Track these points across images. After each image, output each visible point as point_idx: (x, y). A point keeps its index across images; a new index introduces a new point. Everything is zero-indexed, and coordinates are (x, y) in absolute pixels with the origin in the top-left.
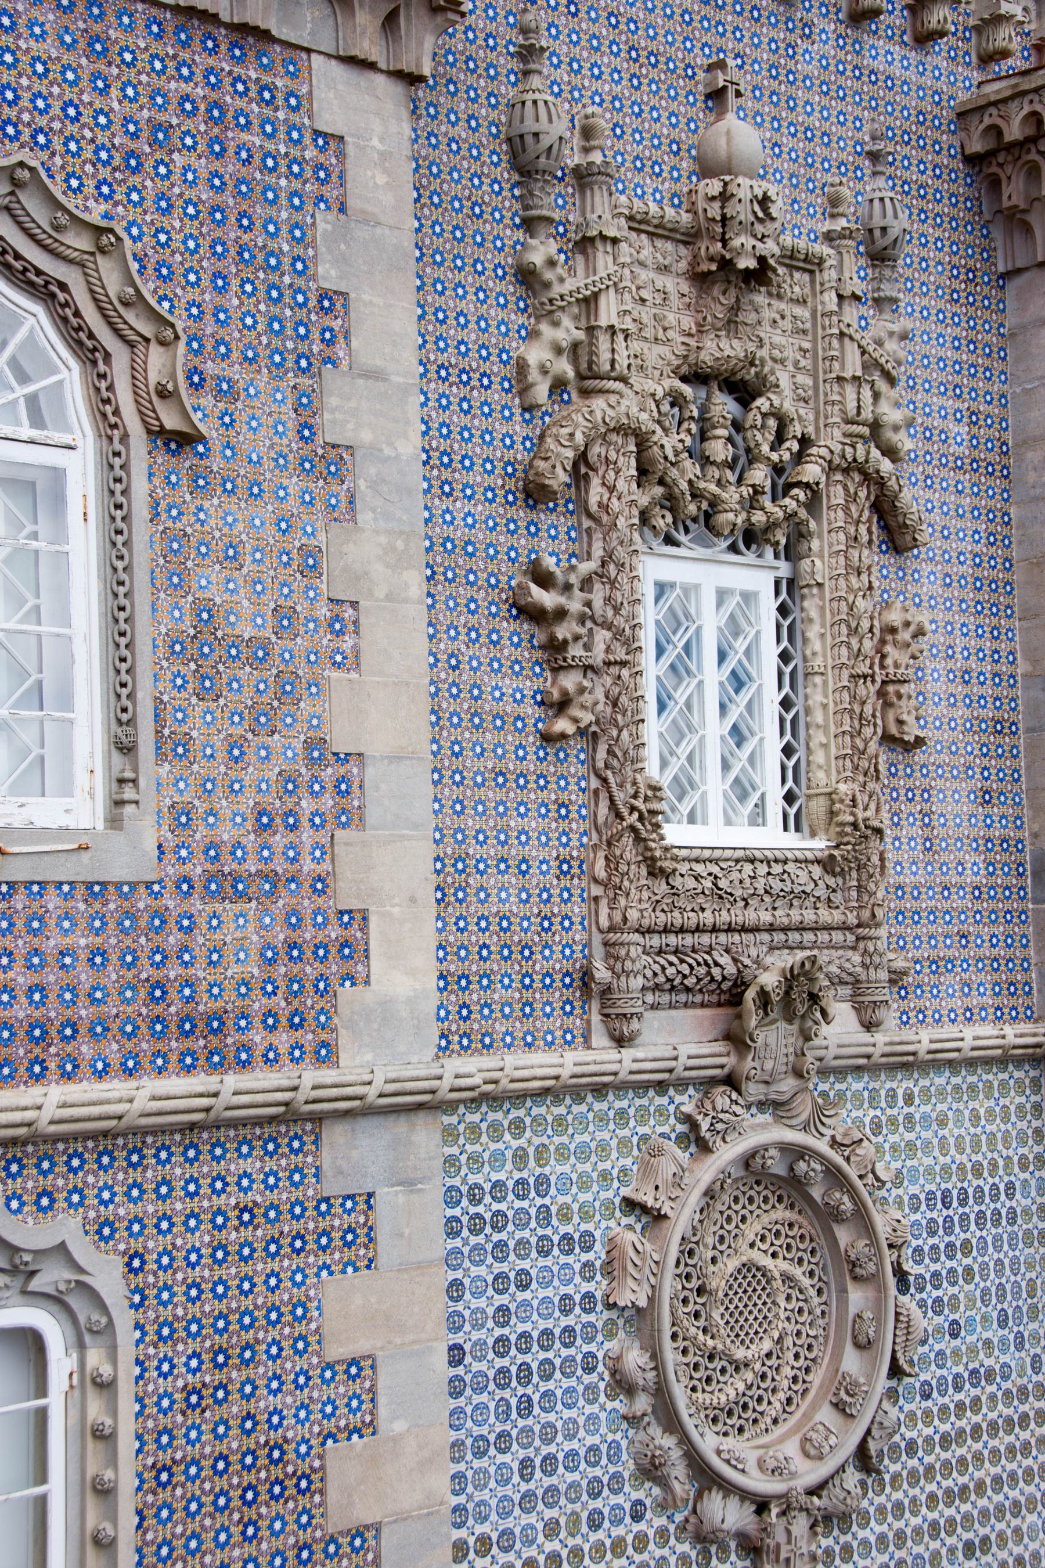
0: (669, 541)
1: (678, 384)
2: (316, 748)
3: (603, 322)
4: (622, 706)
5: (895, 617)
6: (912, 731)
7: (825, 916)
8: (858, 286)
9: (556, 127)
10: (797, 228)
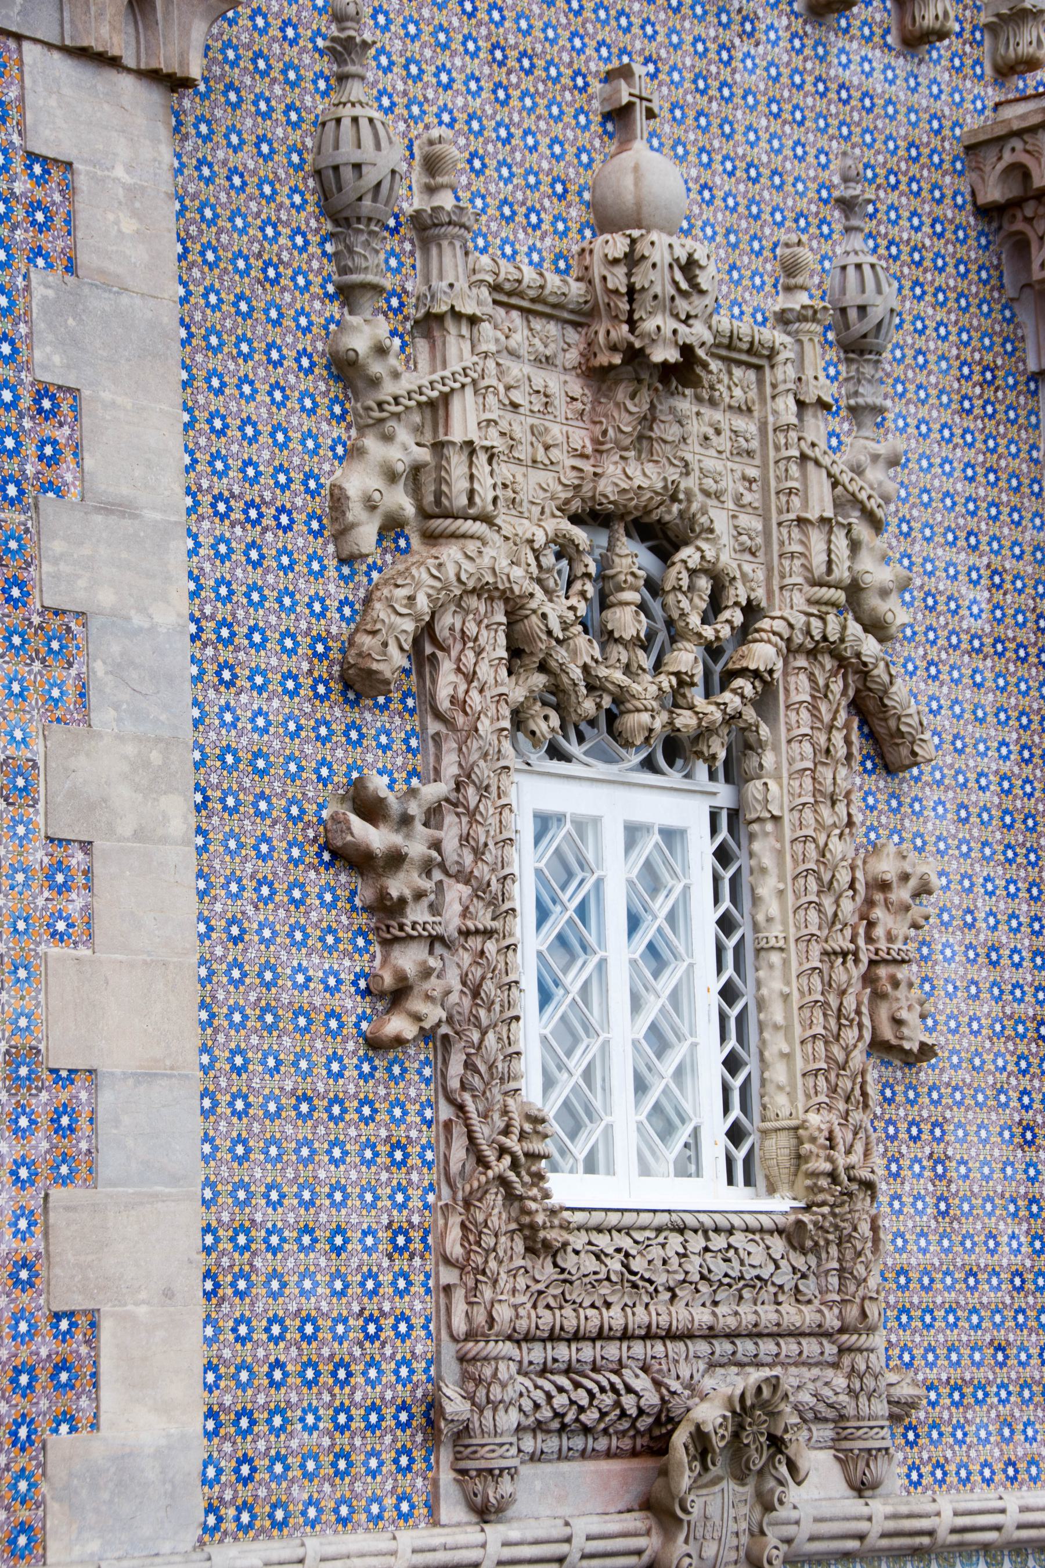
0: (556, 753)
1: (566, 525)
3: (457, 436)
4: (486, 996)
5: (887, 867)
6: (915, 1036)
7: (792, 1315)
8: (827, 391)
9: (385, 156)
10: (737, 304)
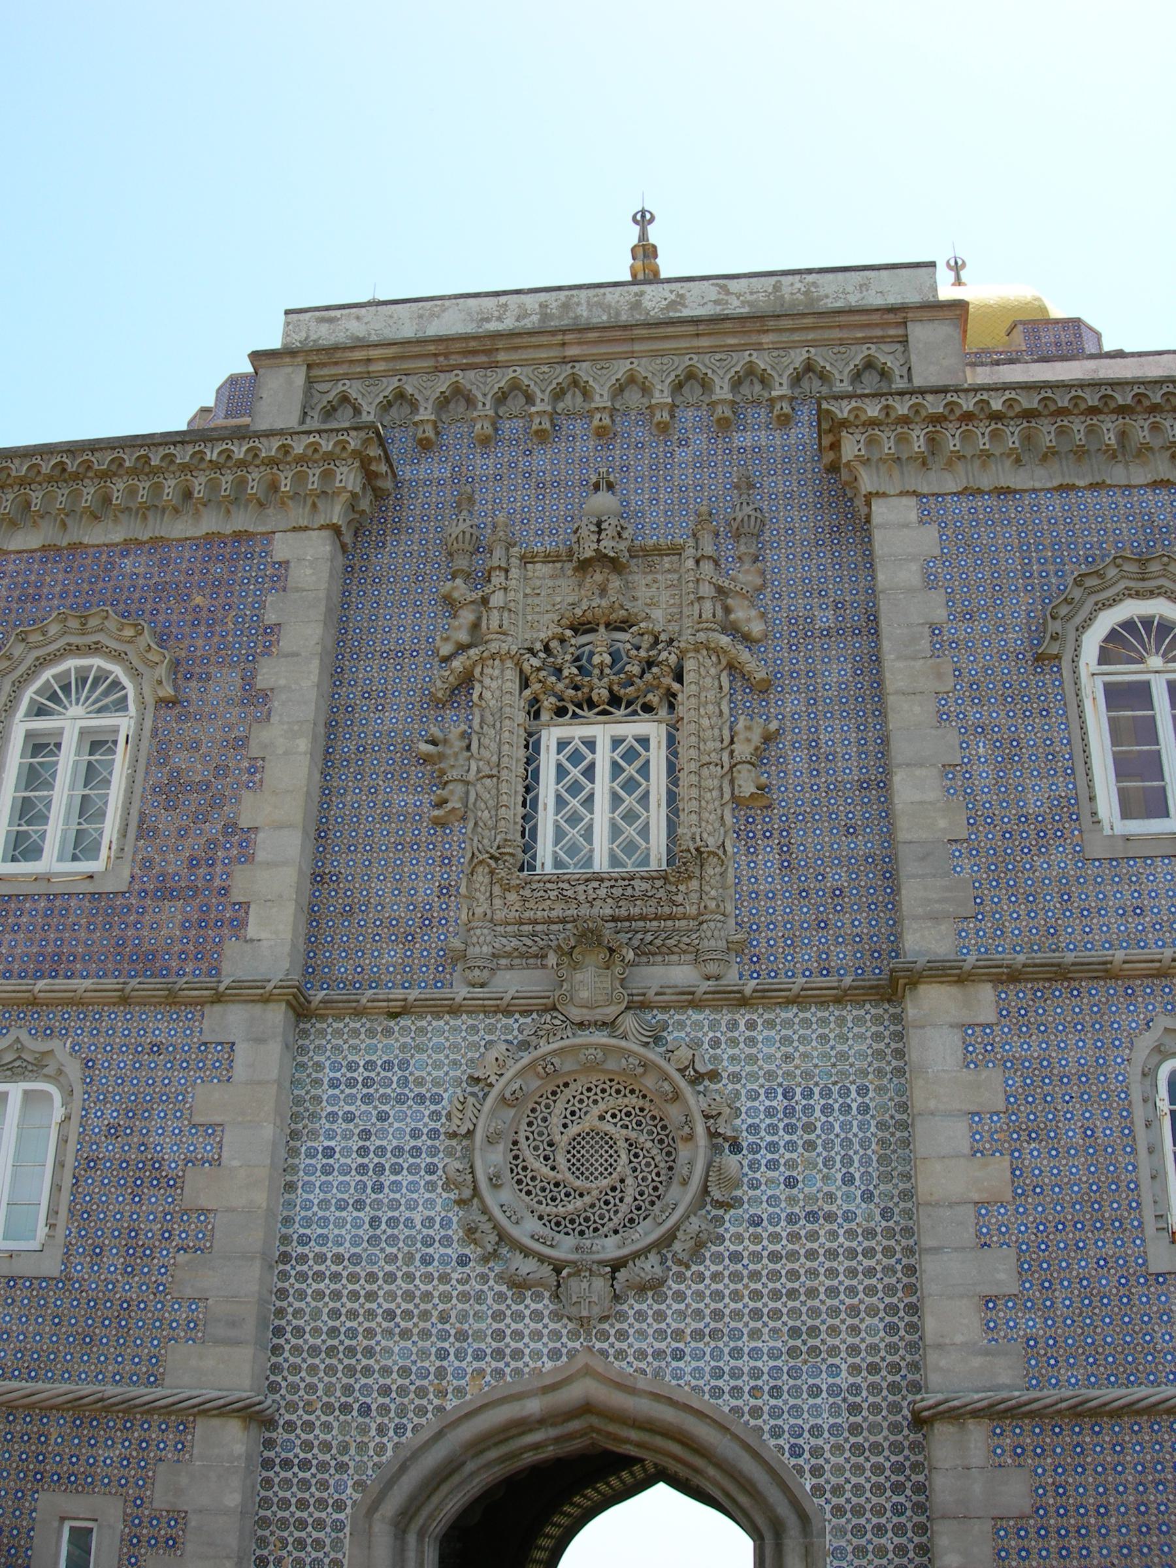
0: (575, 715)
1: (560, 630)
2: (231, 827)
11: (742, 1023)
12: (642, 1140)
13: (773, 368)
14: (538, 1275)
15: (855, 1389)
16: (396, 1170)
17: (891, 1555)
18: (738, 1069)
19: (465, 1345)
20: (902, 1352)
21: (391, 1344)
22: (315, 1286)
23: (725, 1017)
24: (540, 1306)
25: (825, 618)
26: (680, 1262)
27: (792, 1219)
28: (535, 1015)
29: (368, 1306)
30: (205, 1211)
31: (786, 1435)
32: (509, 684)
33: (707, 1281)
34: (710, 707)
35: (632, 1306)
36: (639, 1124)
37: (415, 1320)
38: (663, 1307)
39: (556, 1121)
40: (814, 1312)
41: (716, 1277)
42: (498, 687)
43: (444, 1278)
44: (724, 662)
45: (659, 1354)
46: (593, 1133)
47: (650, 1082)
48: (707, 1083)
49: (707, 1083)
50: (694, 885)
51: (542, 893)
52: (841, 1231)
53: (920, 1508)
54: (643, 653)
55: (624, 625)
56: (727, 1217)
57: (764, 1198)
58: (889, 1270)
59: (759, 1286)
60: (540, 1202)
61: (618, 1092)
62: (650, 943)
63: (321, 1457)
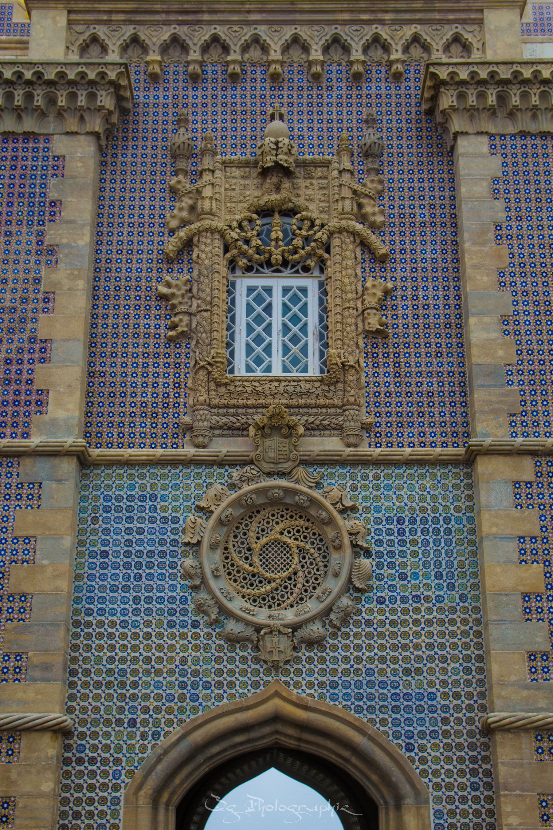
0: (258, 271)
1: (249, 214)
2: (32, 340)
11: (371, 475)
12: (308, 547)
13: (392, 38)
14: (245, 634)
15: (445, 708)
16: (150, 565)
17: (471, 816)
18: (369, 504)
19: (198, 679)
20: (474, 685)
21: (149, 679)
22: (97, 642)
23: (359, 471)
24: (246, 654)
25: (422, 214)
26: (334, 626)
27: (404, 600)
28: (238, 467)
29: (133, 654)
30: (24, 595)
31: (403, 738)
32: (217, 249)
33: (352, 638)
34: (350, 271)
35: (304, 653)
36: (305, 537)
37: (165, 663)
38: (324, 654)
39: (252, 534)
40: (419, 659)
41: (356, 635)
42: (209, 251)
43: (183, 636)
44: (358, 241)
45: (321, 685)
46: (276, 541)
47: (313, 512)
48: (349, 513)
49: (349, 513)
50: (340, 386)
51: (241, 389)
52: (435, 608)
53: (488, 786)
54: (304, 233)
55: (291, 212)
56: (363, 598)
57: (386, 586)
58: (465, 634)
59: (384, 642)
60: (243, 587)
61: (291, 517)
62: (312, 423)
63: (103, 755)
